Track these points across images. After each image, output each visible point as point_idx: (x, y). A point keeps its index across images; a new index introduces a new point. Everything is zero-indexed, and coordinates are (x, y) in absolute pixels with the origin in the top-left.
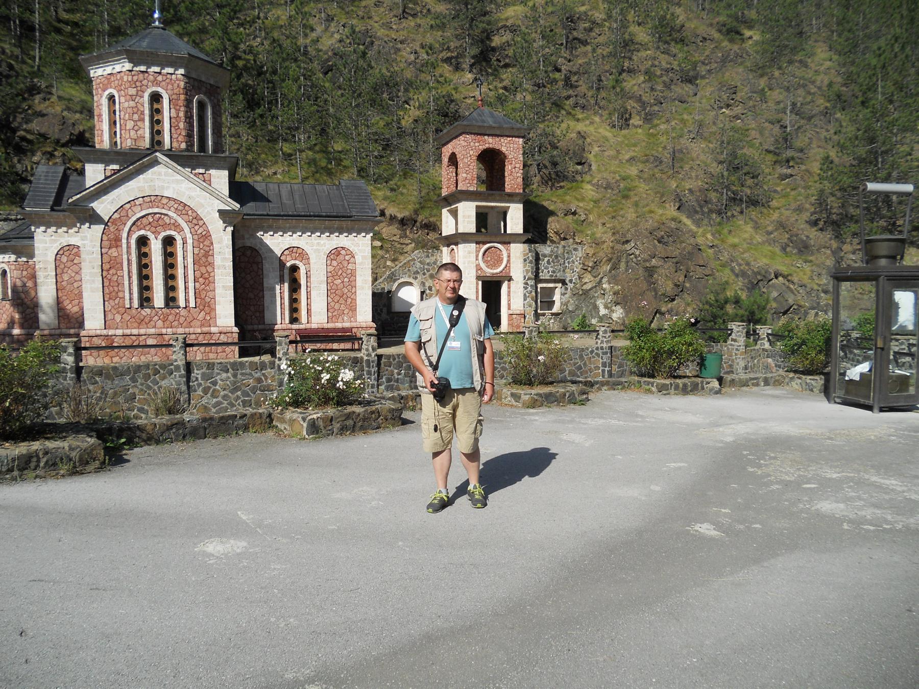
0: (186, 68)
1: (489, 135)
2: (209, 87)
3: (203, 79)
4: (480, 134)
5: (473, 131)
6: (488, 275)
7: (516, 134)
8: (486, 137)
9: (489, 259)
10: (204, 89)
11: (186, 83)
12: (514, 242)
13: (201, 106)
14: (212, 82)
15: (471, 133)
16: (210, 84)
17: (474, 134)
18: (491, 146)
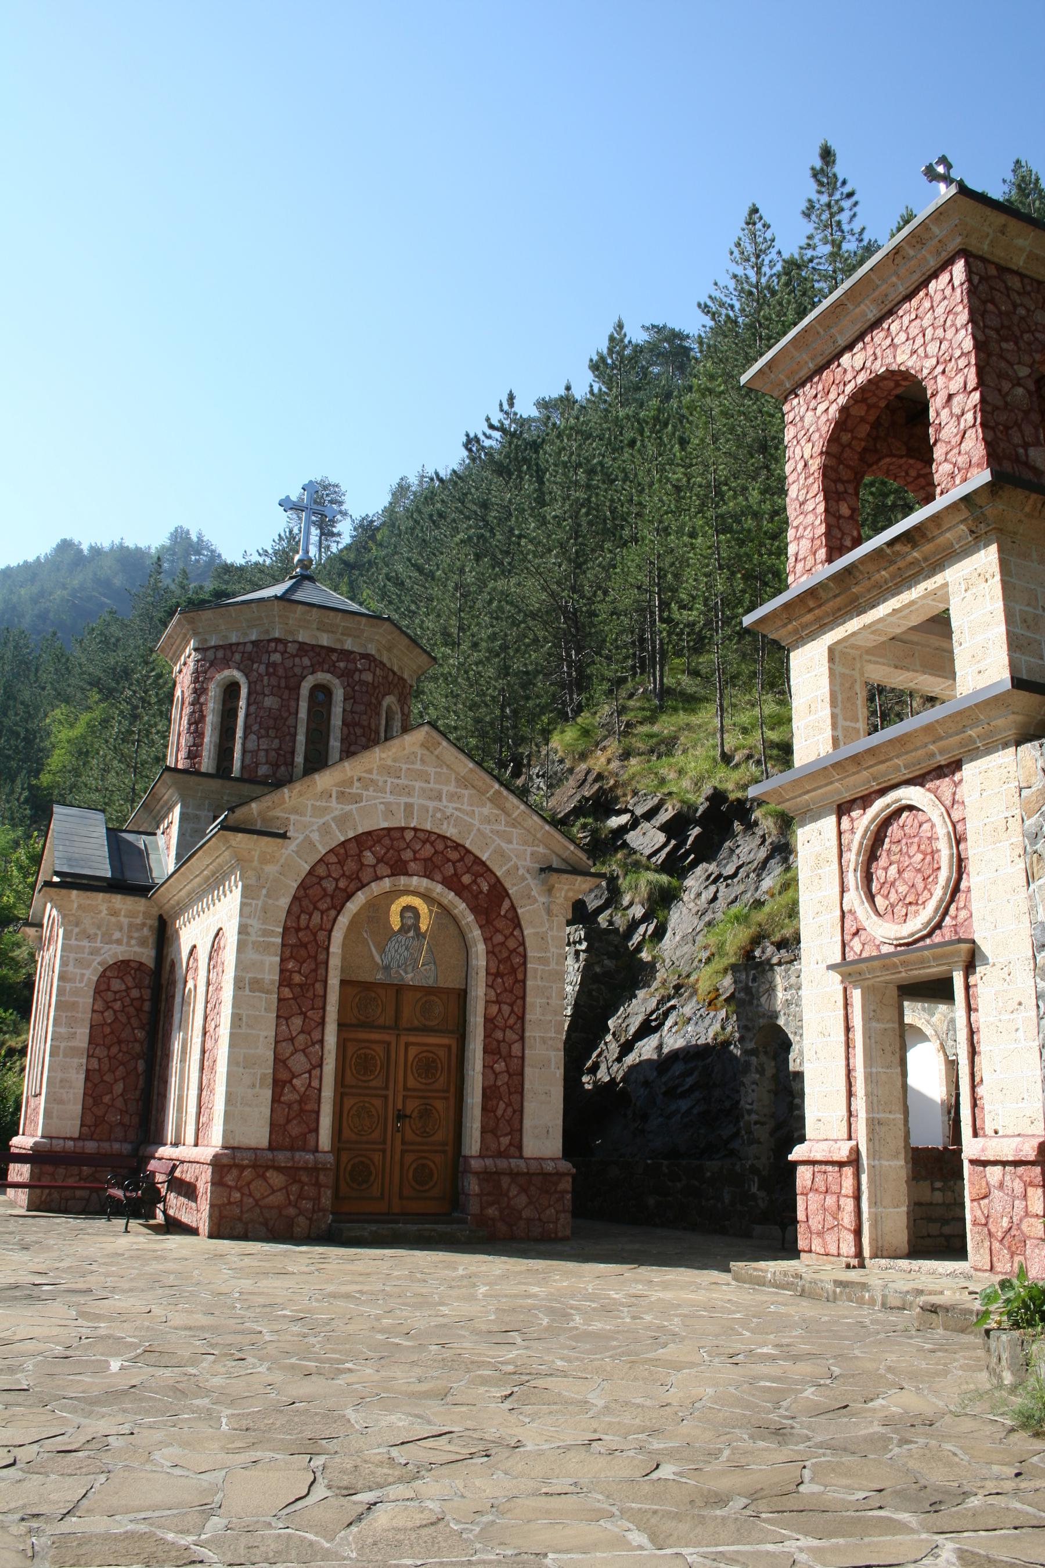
0: (195, 634)
1: (850, 347)
2: (249, 648)
3: (234, 640)
4: (827, 365)
5: (804, 373)
6: (886, 949)
7: (933, 263)
8: (846, 359)
9: (893, 870)
10: (237, 657)
11: (198, 661)
12: (975, 753)
13: (231, 690)
14: (254, 638)
15: (803, 385)
16: (252, 642)
17: (809, 379)
18: (862, 378)
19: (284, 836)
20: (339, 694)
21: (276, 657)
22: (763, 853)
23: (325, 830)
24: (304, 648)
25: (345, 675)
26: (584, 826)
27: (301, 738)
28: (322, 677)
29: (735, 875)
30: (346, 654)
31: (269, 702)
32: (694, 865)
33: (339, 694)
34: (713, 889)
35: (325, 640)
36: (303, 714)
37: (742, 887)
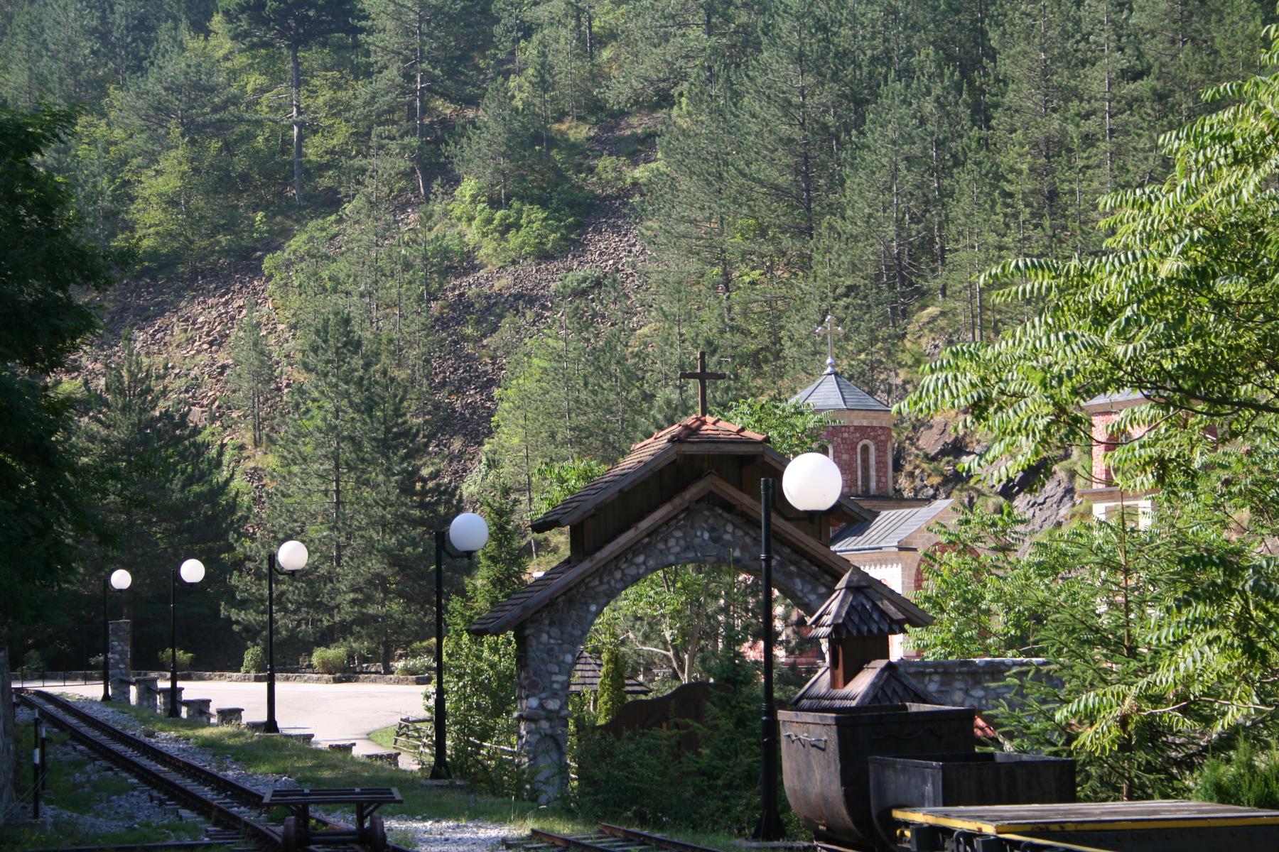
19: (915, 550)
20: (872, 449)
21: (846, 435)
22: (1060, 491)
23: (924, 544)
24: (858, 428)
25: (874, 438)
26: (948, 463)
27: (859, 473)
28: (865, 441)
29: (1044, 503)
30: (873, 428)
31: (845, 457)
32: (1018, 492)
33: (872, 449)
34: (1032, 510)
35: (865, 423)
36: (859, 461)
37: (1049, 513)
